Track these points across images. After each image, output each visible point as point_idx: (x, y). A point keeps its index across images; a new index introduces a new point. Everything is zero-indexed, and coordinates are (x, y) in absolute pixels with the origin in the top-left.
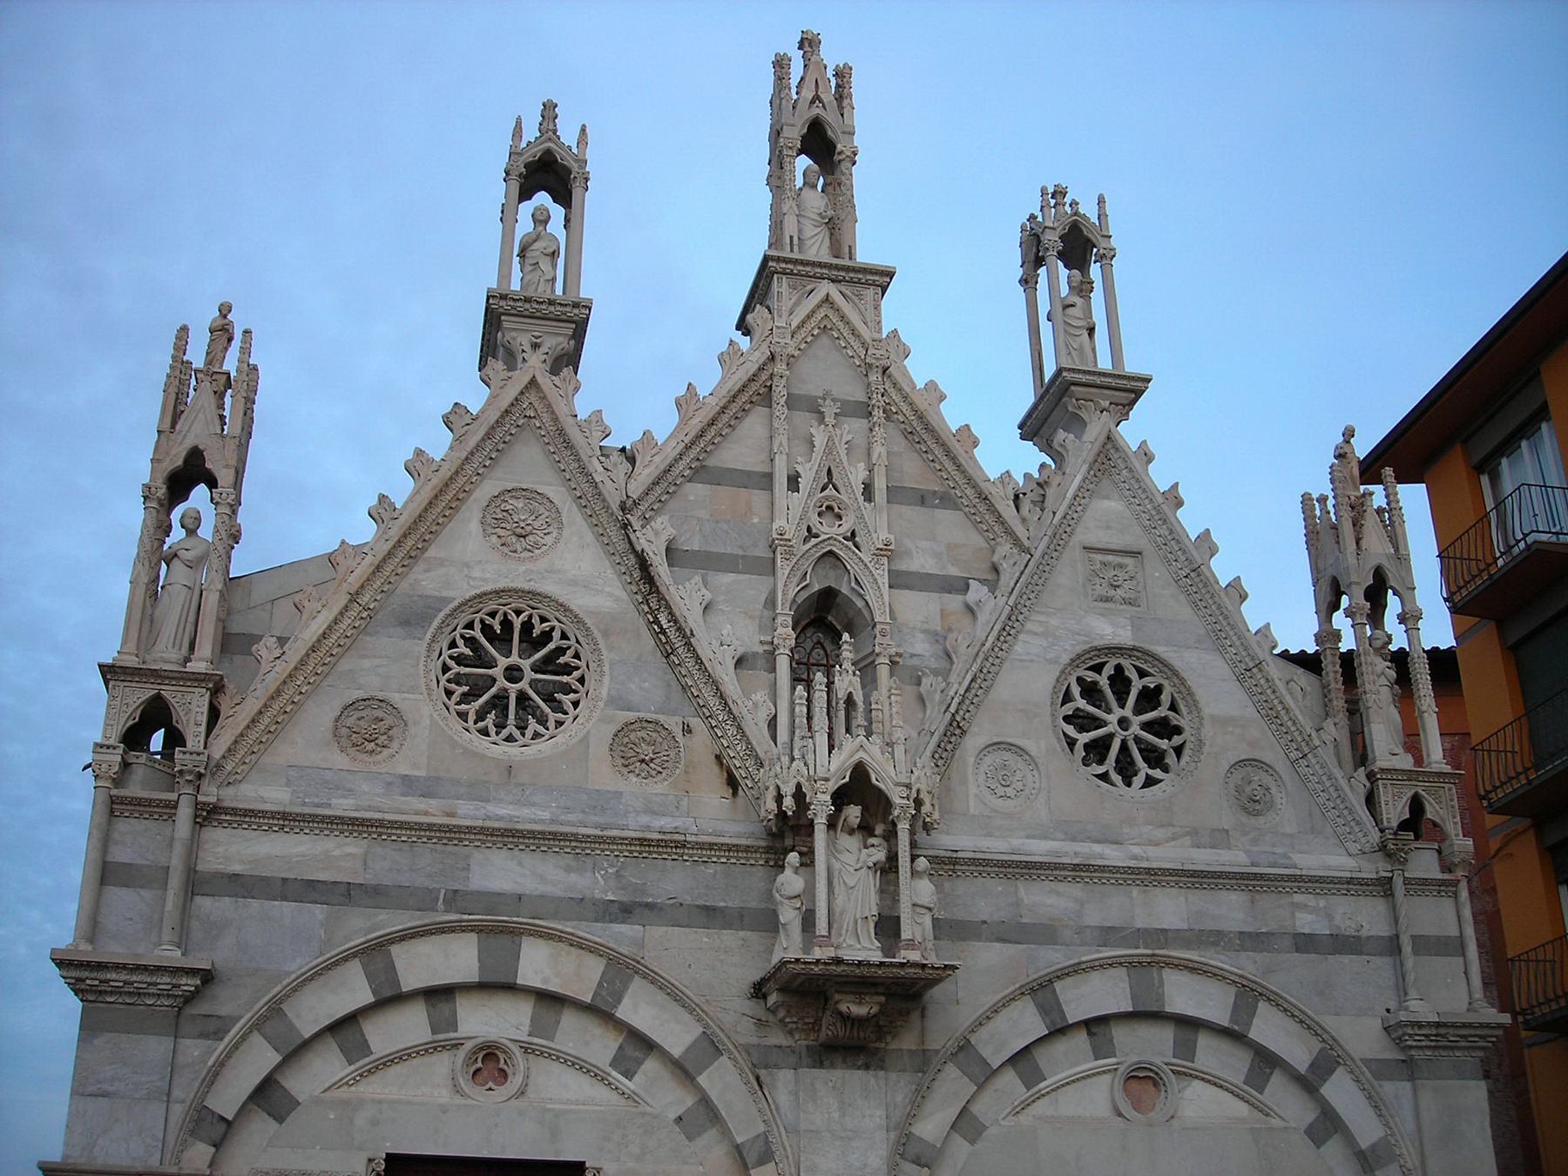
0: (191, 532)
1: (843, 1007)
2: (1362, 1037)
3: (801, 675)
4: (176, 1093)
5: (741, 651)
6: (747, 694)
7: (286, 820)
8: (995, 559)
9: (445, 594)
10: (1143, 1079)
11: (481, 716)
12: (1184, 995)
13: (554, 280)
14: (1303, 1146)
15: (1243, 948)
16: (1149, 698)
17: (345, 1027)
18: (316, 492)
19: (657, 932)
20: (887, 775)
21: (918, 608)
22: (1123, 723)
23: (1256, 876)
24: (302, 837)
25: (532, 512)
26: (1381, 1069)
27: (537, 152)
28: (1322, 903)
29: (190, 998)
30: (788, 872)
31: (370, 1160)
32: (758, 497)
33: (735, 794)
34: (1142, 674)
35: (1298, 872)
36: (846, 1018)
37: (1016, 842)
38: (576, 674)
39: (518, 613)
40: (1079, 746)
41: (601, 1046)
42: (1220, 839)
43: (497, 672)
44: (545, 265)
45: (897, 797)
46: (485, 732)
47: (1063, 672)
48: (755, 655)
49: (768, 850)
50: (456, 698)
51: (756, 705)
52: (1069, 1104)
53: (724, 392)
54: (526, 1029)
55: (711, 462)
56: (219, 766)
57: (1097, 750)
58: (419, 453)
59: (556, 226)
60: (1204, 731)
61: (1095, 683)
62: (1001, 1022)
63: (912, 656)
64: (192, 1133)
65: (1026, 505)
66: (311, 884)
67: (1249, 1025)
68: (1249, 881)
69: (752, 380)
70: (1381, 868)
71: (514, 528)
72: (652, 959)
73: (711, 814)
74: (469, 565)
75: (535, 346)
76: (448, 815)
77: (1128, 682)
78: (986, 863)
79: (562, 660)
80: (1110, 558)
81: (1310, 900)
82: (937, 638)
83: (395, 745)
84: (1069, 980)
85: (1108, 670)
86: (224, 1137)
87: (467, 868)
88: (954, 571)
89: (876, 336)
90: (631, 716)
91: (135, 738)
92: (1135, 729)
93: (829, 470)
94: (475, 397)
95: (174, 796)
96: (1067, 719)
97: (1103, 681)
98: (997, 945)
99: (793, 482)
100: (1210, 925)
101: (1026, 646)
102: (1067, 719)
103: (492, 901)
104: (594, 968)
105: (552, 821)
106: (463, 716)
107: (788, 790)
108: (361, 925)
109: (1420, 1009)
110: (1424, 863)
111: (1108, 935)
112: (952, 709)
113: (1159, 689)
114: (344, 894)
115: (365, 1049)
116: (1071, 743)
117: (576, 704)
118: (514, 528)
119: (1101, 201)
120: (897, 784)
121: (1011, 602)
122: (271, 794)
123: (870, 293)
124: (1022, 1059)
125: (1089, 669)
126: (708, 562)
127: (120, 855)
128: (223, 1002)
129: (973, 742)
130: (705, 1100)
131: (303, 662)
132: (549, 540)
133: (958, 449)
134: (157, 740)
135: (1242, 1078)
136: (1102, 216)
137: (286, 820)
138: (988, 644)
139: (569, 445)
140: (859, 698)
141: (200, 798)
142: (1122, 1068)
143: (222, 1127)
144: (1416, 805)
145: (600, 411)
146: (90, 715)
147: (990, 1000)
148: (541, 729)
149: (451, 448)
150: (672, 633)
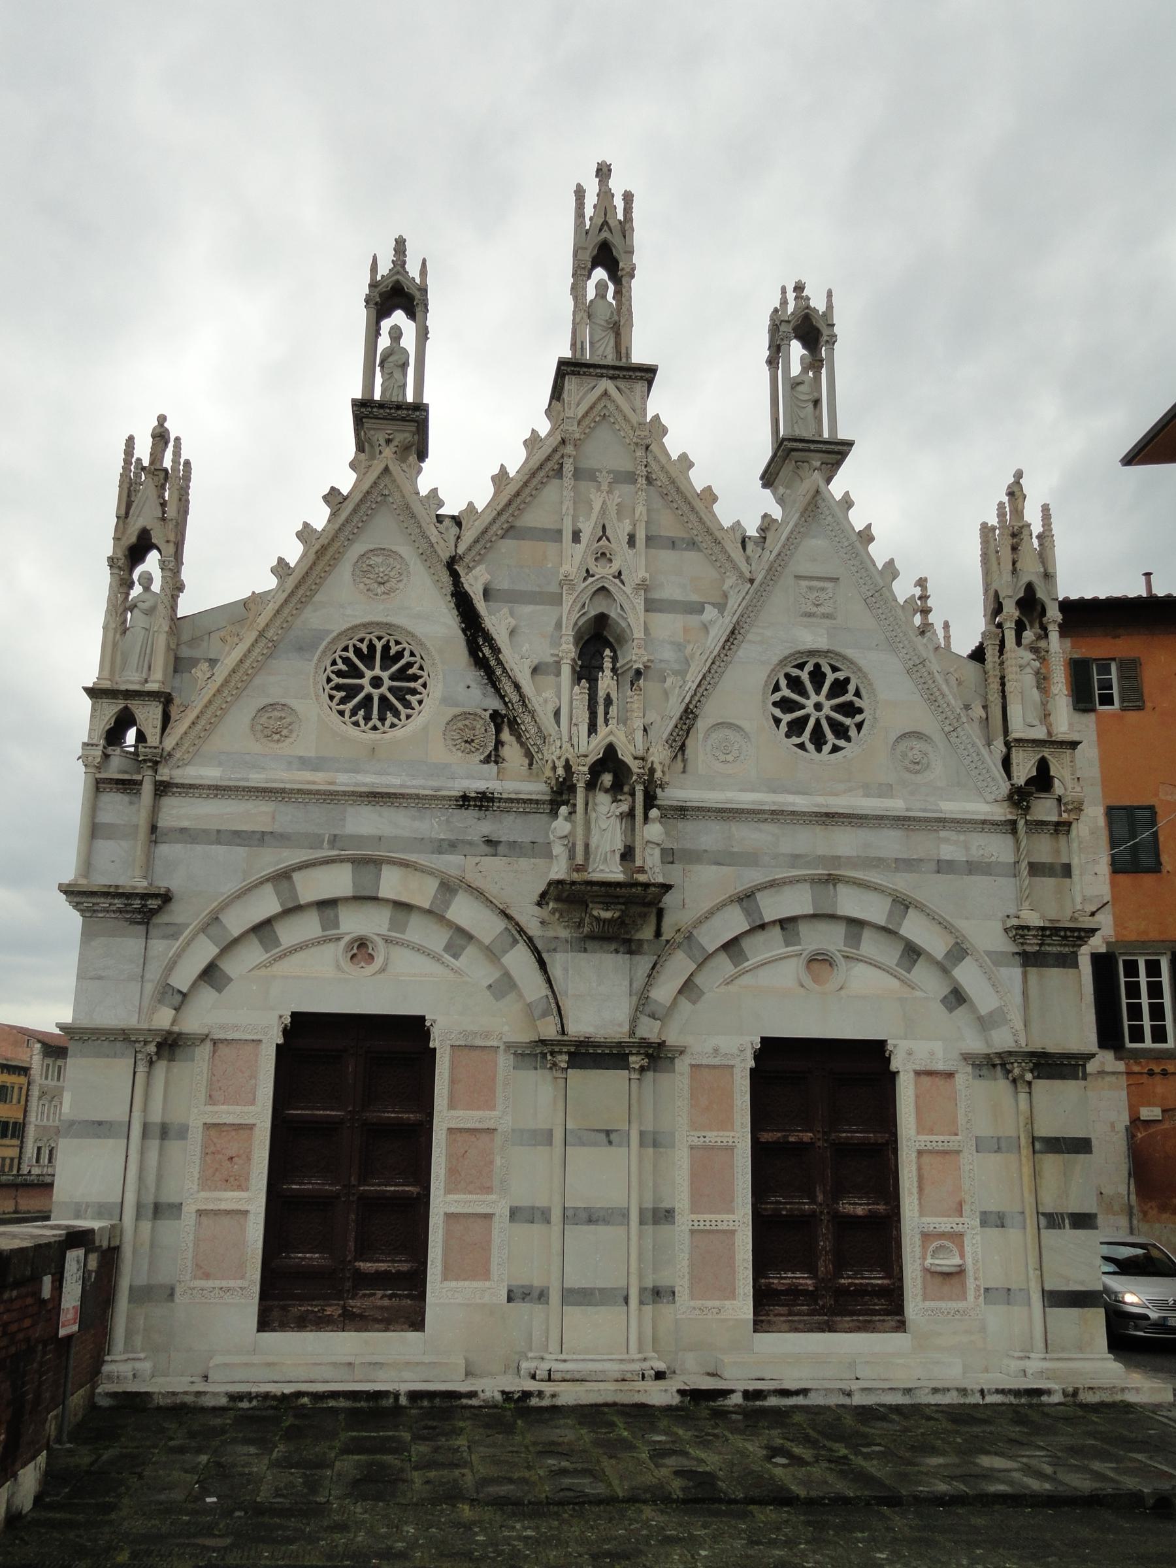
0: (147, 588)
1: (595, 913)
2: (989, 936)
3: (578, 677)
4: (147, 976)
5: (536, 662)
6: (539, 692)
7: (218, 791)
8: (725, 587)
9: (328, 627)
10: (819, 961)
11: (354, 713)
12: (850, 903)
13: (405, 385)
14: (939, 1009)
15: (897, 869)
16: (840, 687)
17: (263, 929)
18: (231, 558)
19: (471, 860)
20: (625, 754)
21: (667, 625)
22: (818, 707)
23: (909, 818)
24: (230, 801)
25: (388, 565)
26: (998, 959)
27: (389, 283)
28: (962, 838)
29: (154, 912)
30: (560, 819)
31: (281, 1017)
32: (551, 547)
33: (531, 764)
34: (835, 669)
35: (943, 816)
36: (598, 919)
37: (730, 795)
38: (421, 681)
39: (380, 638)
40: (783, 725)
41: (437, 938)
42: (885, 791)
43: (365, 681)
44: (397, 374)
45: (634, 766)
46: (356, 724)
47: (773, 670)
48: (547, 664)
49: (551, 802)
50: (336, 700)
51: (546, 701)
52: (765, 977)
53: (526, 470)
54: (386, 926)
55: (518, 523)
56: (170, 755)
57: (796, 727)
58: (306, 525)
59: (408, 342)
60: (878, 712)
61: (798, 677)
62: (716, 921)
63: (661, 661)
64: (160, 1001)
65: (750, 546)
66: (236, 833)
67: (900, 925)
68: (903, 822)
69: (548, 459)
71: (378, 578)
72: (470, 877)
73: (515, 779)
74: (346, 608)
75: (388, 441)
76: (330, 784)
77: (824, 675)
78: (709, 810)
79: (410, 672)
80: (815, 583)
81: (952, 835)
82: (679, 647)
83: (294, 735)
84: (766, 892)
85: (809, 667)
86: (182, 1002)
87: (344, 820)
88: (694, 598)
89: (641, 421)
90: (457, 710)
91: (114, 736)
92: (826, 710)
93: (604, 527)
94: (346, 481)
95: (139, 777)
96: (775, 704)
97: (805, 676)
98: (714, 867)
99: (576, 536)
100: (874, 853)
101: (745, 651)
102: (775, 704)
103: (360, 840)
104: (432, 885)
105: (401, 786)
106: (342, 713)
107: (560, 764)
108: (272, 860)
111: (795, 859)
112: (687, 700)
113: (847, 681)
114: (261, 839)
115: (276, 942)
116: (777, 721)
117: (420, 702)
118: (378, 578)
119: (830, 294)
120: (635, 758)
121: (734, 620)
122: (209, 773)
123: (640, 386)
124: (732, 947)
125: (794, 667)
126: (515, 597)
127: (105, 817)
128: (178, 913)
129: (701, 725)
130: (507, 975)
131: (226, 682)
132: (401, 585)
133: (699, 505)
134: (131, 736)
135: (895, 962)
136: (830, 306)
137: (218, 791)
138: (715, 653)
139: (413, 516)
140: (614, 696)
141: (158, 778)
142: (805, 953)
143: (179, 998)
145: (436, 489)
146: (79, 718)
147: (706, 906)
148: (396, 721)
149: (329, 521)
150: (487, 651)
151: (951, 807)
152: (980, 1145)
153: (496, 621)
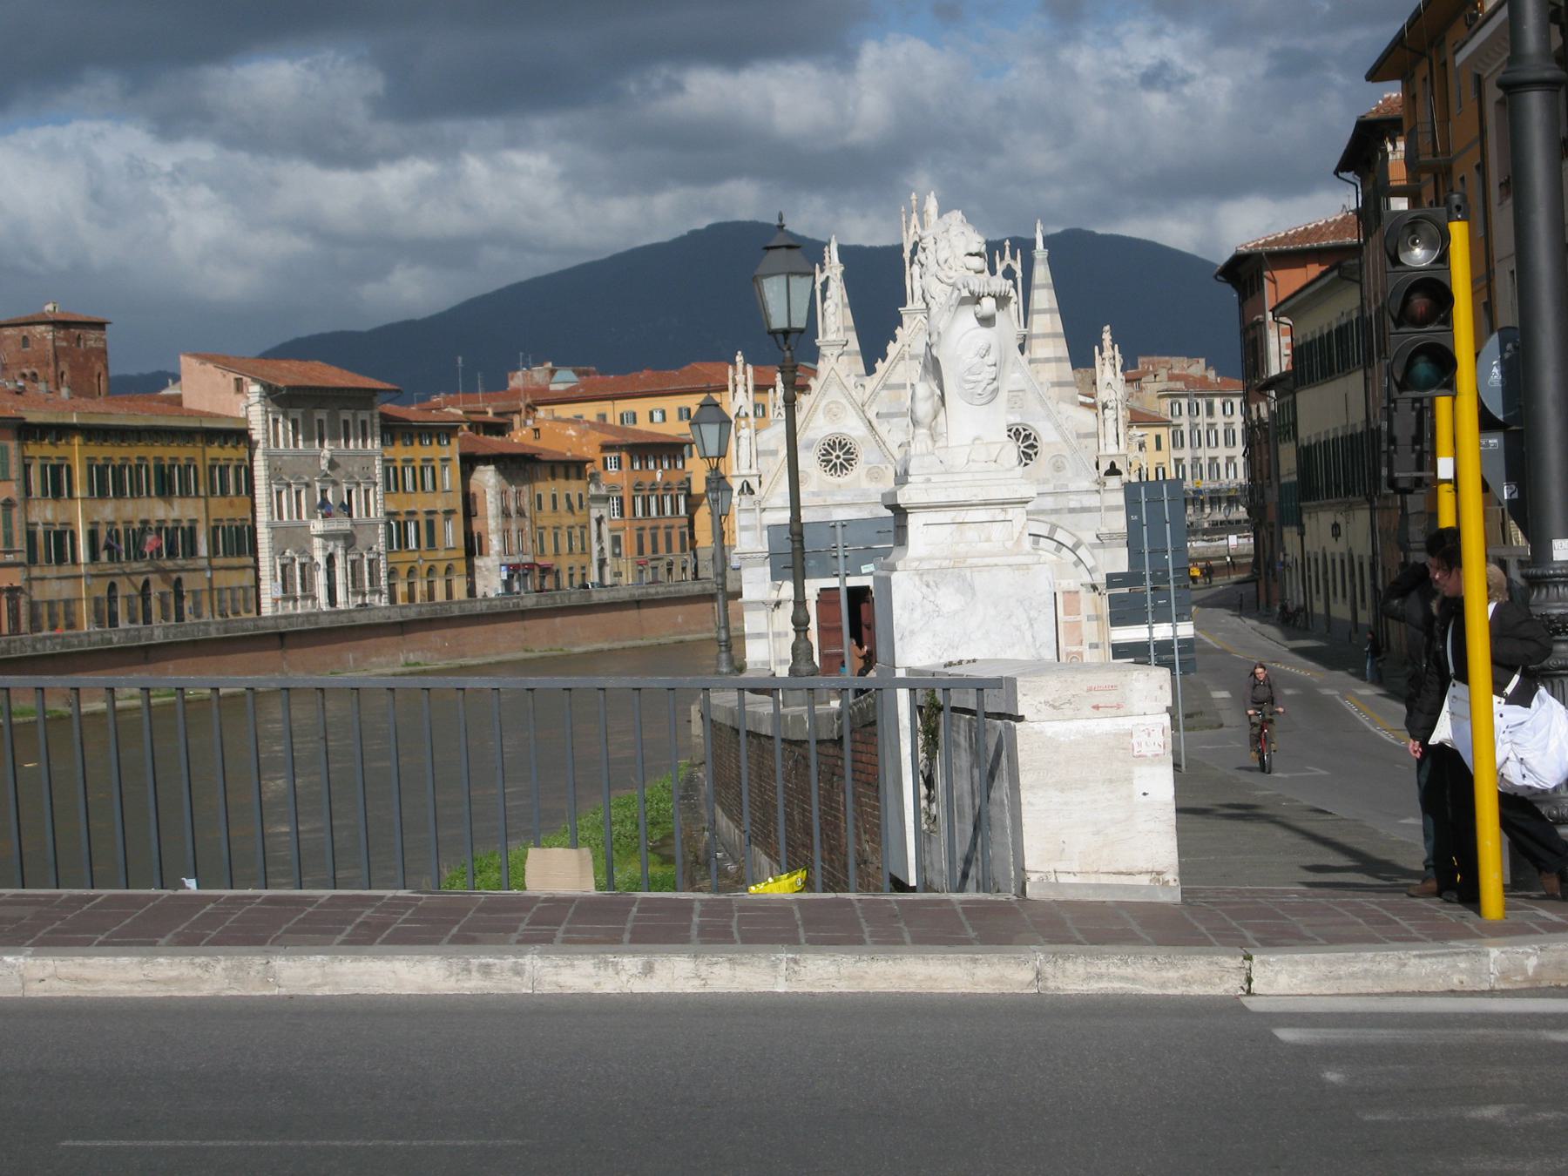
2: (1089, 537)
16: (1027, 437)
26: (1093, 546)
42: (1046, 482)
70: (1096, 487)
109: (1104, 530)
110: (1114, 482)
118: (832, 415)
144: (1113, 465)
151: (1072, 487)
152: (1089, 618)
153: (882, 428)
